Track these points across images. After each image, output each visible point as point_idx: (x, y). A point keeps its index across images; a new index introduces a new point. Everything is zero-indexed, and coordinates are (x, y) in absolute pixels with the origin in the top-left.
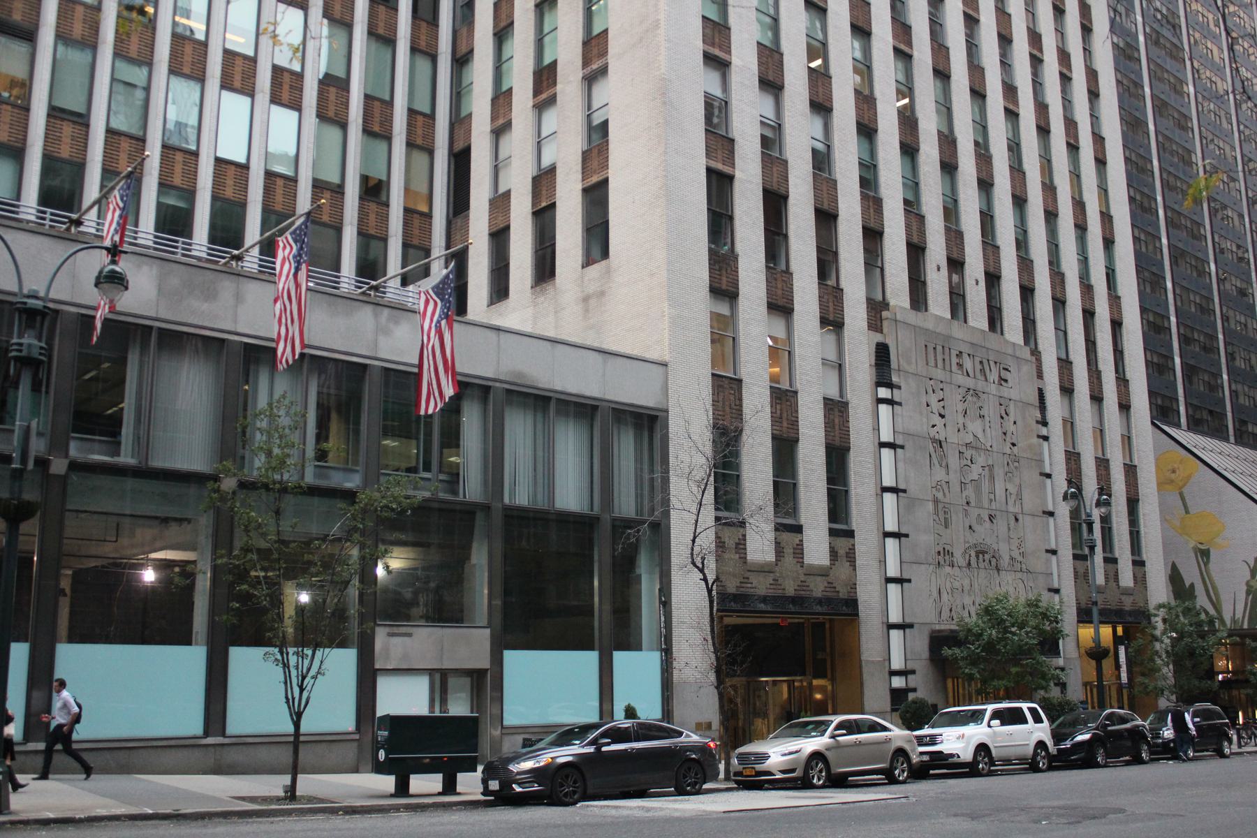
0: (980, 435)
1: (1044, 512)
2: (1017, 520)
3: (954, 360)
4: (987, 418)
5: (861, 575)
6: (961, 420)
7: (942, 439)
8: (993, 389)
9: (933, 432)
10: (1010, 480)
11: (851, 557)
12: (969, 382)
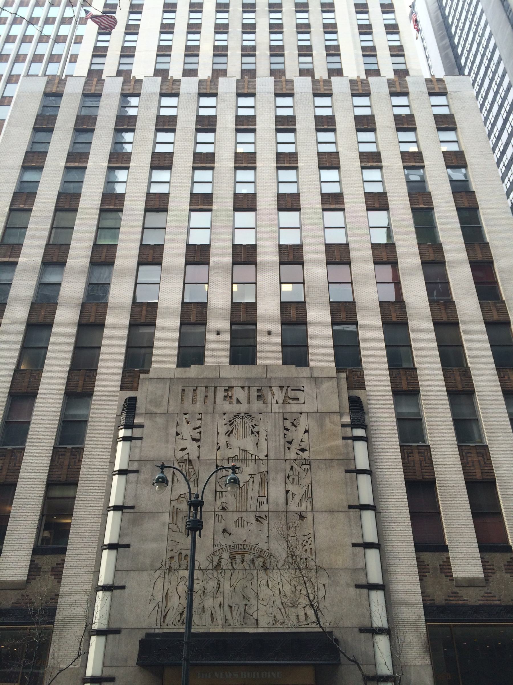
0: (250, 447)
1: (350, 507)
2: (302, 517)
3: (220, 394)
4: (263, 434)
5: (66, 586)
6: (223, 439)
7: (193, 457)
8: (276, 408)
9: (179, 455)
10: (294, 482)
11: (57, 572)
12: (243, 408)
